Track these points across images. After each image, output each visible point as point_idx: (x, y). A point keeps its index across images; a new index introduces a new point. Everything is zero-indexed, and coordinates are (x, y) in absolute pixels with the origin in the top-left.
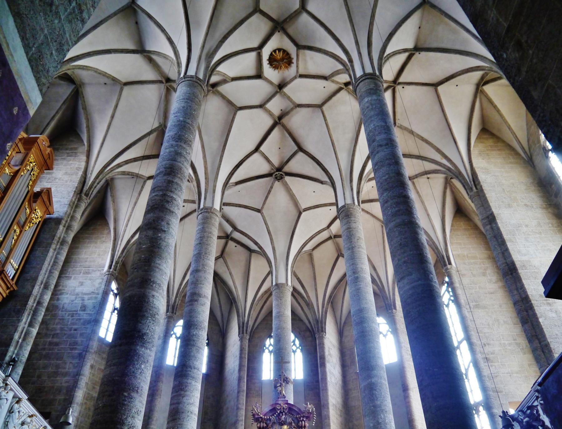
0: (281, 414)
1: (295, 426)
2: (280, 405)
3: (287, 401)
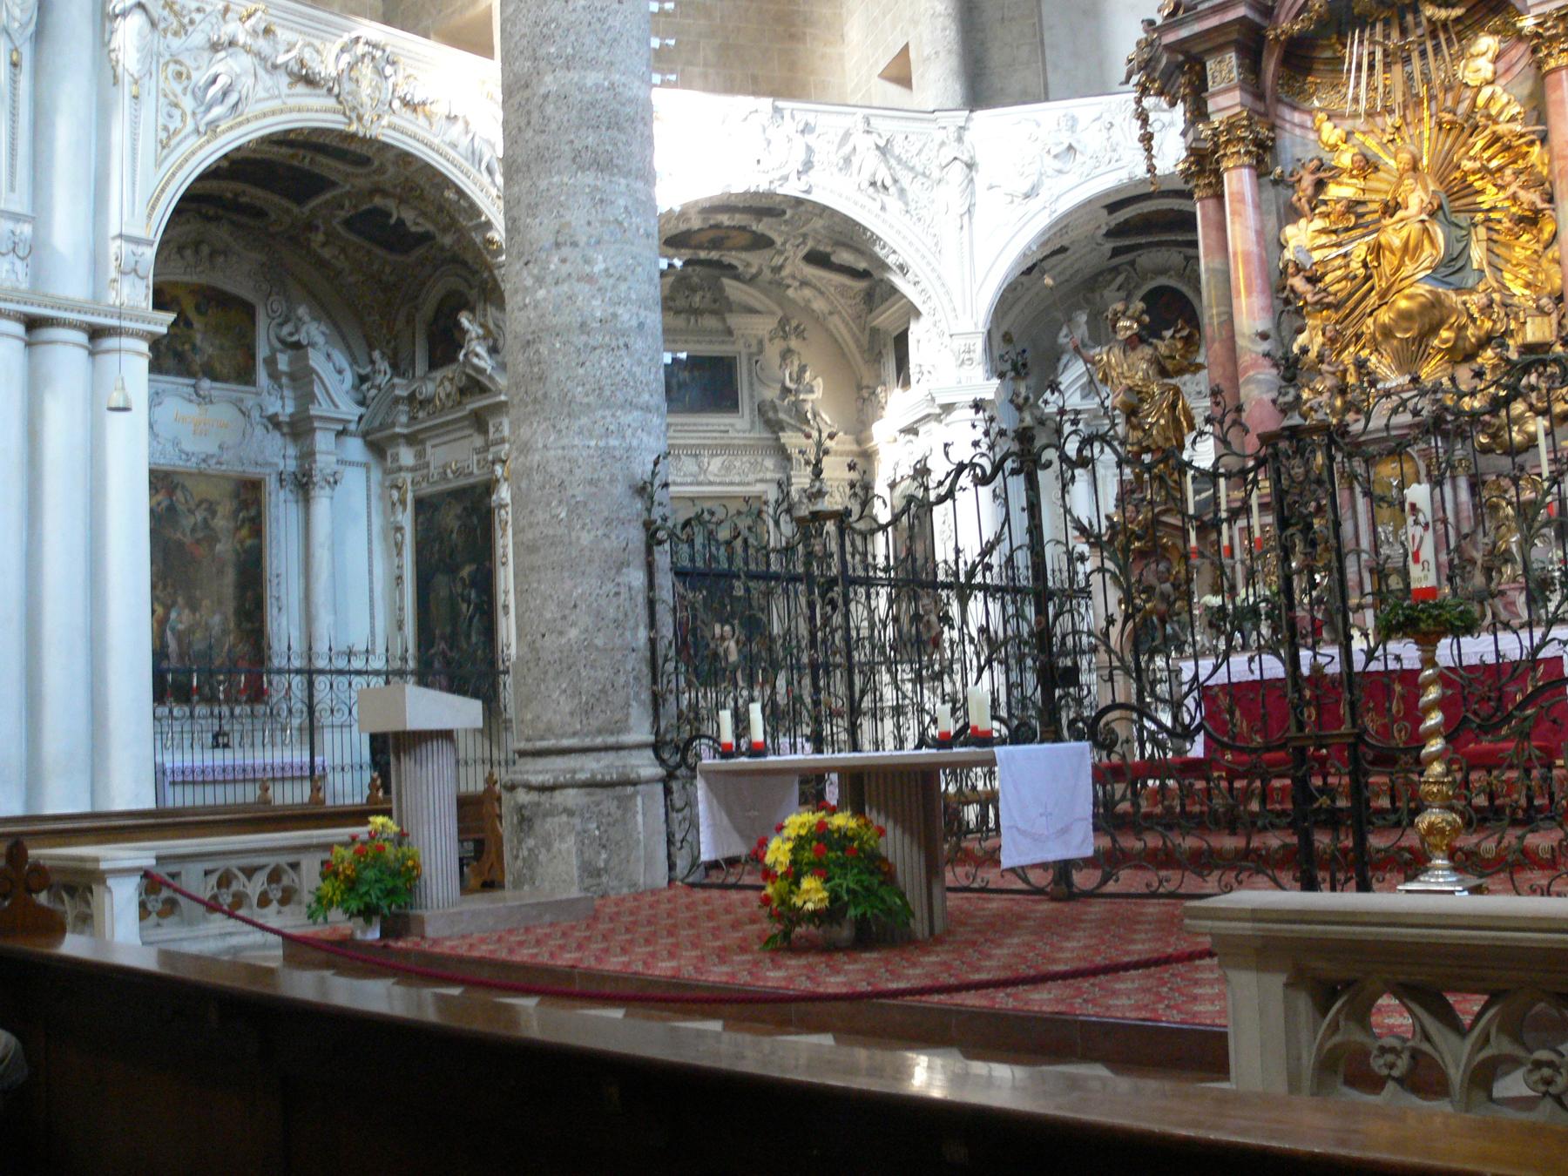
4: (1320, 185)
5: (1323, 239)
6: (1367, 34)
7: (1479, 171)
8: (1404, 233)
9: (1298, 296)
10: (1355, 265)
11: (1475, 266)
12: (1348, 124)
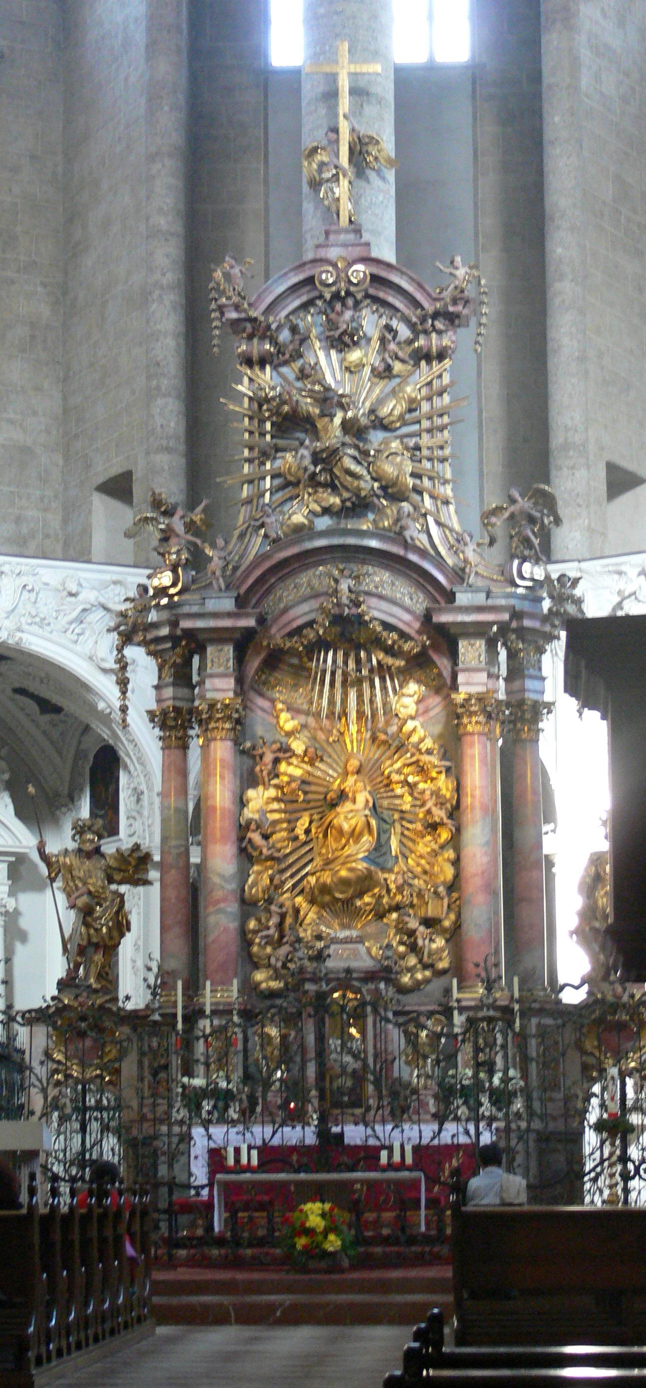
0: (338, 307)
1: (400, 354)
3: (368, 244)
4: (276, 761)
5: (275, 806)
7: (401, 782)
8: (353, 822)
9: (255, 848)
10: (300, 831)
11: (393, 853)
12: (302, 719)
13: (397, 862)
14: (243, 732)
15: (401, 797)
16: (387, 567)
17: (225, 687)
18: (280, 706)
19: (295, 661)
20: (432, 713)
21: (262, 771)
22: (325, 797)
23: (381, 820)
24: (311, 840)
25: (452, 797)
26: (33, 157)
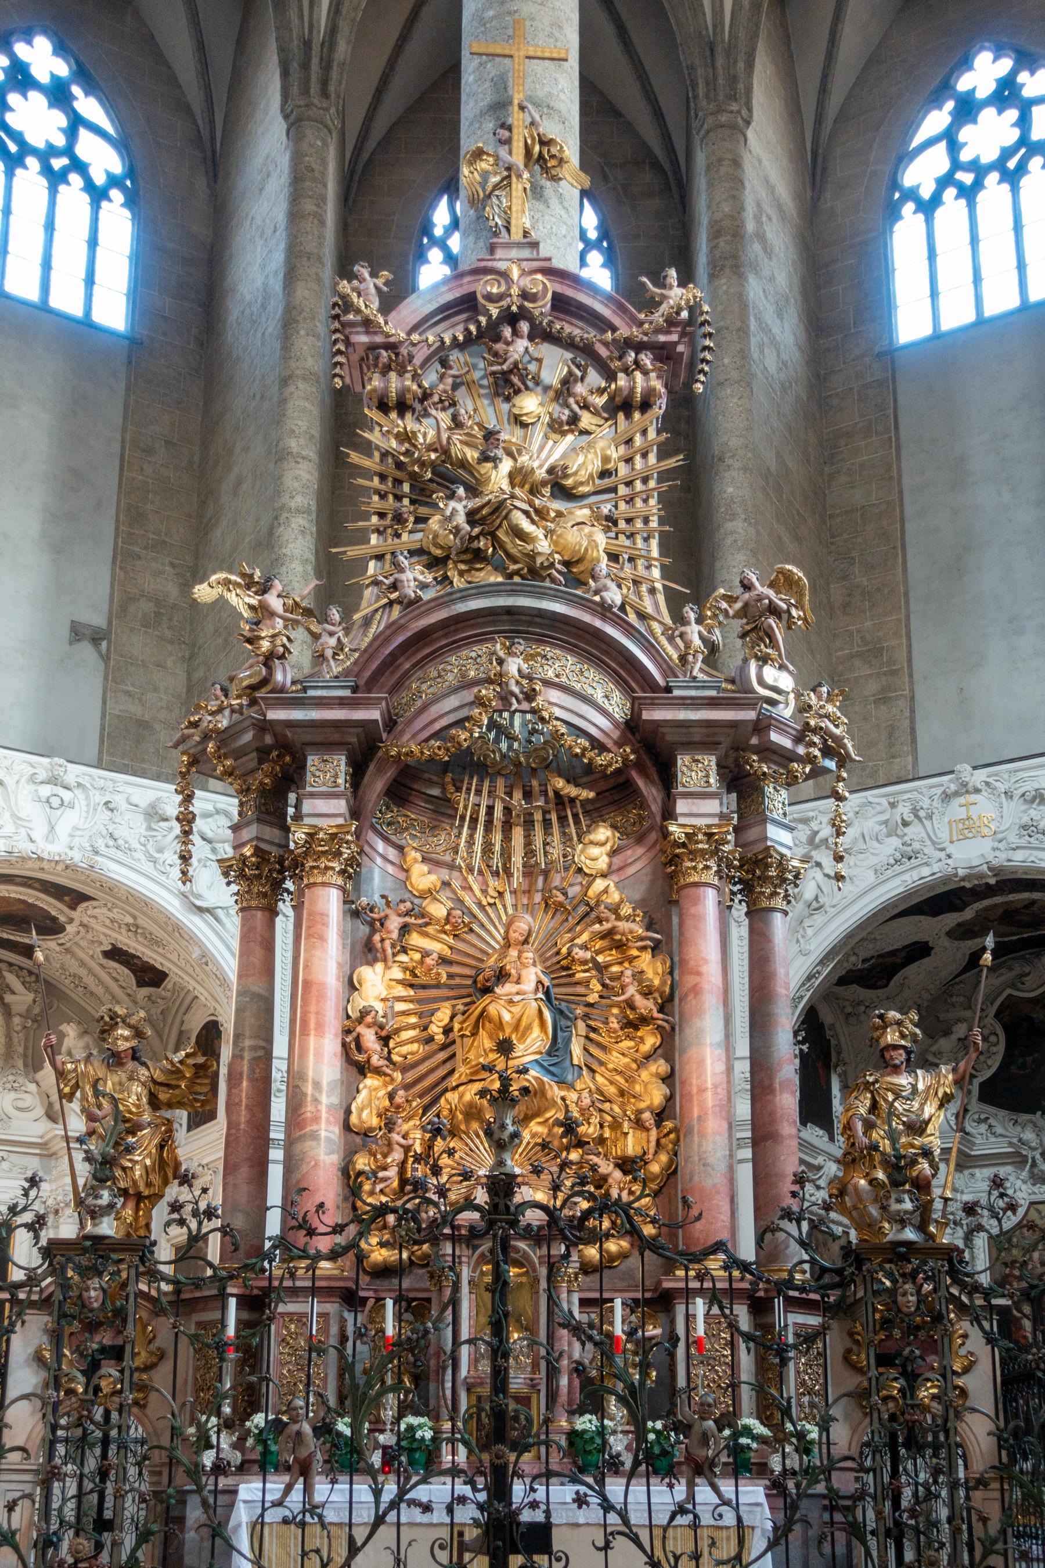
2: (505, 275)
5: (401, 991)
6: (486, 784)
10: (435, 1029)
13: (580, 1075)
14: (357, 888)
15: (586, 983)
16: (572, 648)
17: (332, 811)
18: (413, 855)
19: (436, 792)
20: (631, 870)
21: (382, 940)
22: (475, 982)
23: (558, 1013)
24: (454, 1042)
25: (663, 983)
26: (168, 443)
